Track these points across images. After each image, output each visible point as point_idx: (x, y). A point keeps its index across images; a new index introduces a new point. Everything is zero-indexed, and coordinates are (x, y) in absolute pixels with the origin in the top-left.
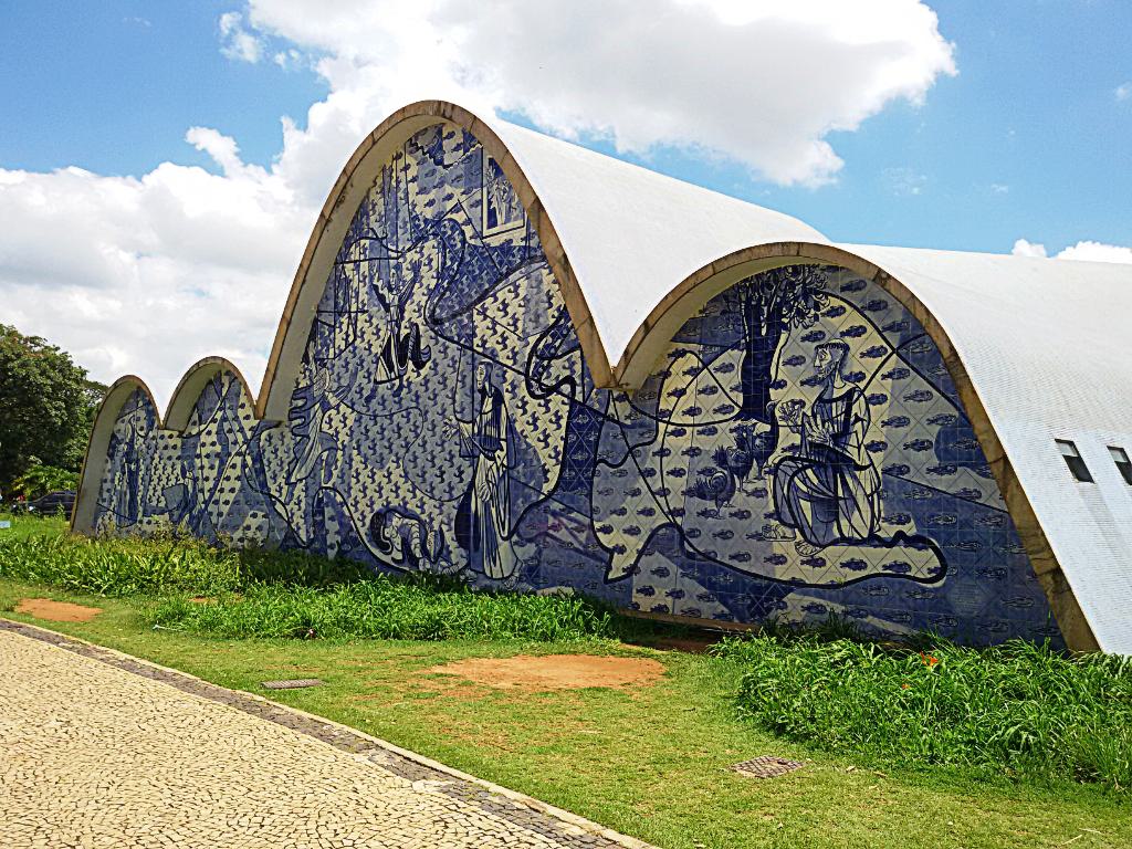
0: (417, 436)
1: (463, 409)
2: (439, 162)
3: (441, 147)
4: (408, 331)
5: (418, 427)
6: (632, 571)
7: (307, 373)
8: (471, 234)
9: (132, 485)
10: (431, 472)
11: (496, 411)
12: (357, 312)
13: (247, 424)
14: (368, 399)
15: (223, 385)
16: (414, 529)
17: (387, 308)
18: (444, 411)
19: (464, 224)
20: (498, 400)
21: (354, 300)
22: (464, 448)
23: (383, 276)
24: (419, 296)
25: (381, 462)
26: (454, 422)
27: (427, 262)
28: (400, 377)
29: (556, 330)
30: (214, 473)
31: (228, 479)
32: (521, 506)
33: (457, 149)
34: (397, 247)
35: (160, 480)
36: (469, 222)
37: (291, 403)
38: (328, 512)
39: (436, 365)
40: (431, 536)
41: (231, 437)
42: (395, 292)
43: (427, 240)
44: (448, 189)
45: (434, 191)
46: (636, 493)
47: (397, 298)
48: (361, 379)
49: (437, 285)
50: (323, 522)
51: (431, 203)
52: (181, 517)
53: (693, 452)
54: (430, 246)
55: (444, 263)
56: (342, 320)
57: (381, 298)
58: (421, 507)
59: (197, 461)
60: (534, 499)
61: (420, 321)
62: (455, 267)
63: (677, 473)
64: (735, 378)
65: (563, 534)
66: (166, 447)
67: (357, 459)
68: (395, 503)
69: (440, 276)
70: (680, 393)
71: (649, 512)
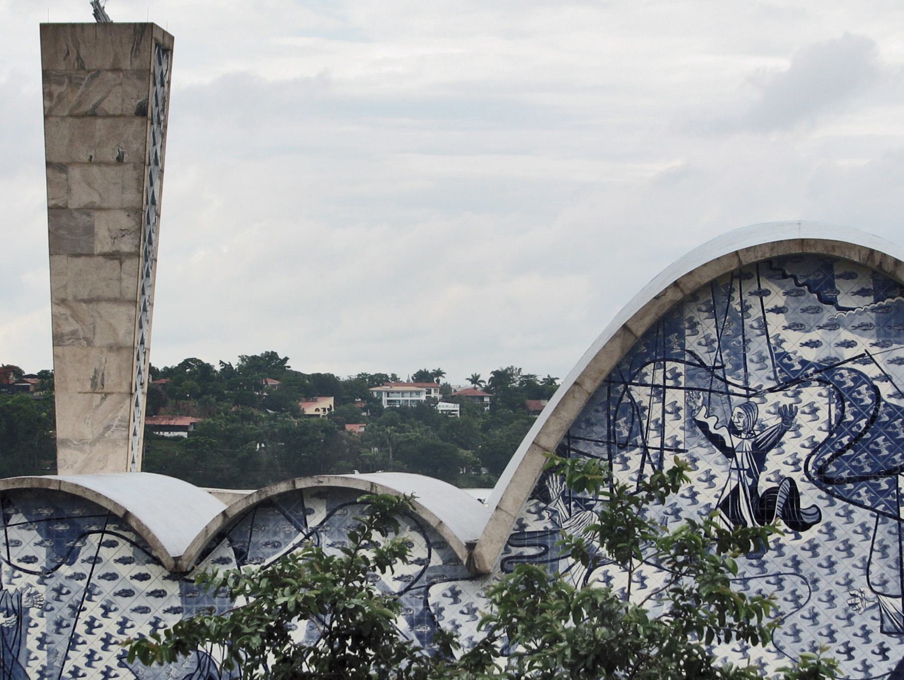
0: (799, 607)
1: (884, 583)
2: (833, 302)
3: (832, 286)
4: (776, 485)
5: (799, 597)
7: (545, 513)
8: (891, 392)
12: (662, 448)
15: (311, 512)
17: (729, 453)
18: (851, 581)
19: (876, 378)
21: (652, 434)
22: (888, 623)
23: (718, 411)
24: (793, 445)
26: (869, 594)
27: (807, 410)
33: (863, 292)
34: (746, 382)
36: (887, 378)
37: (507, 550)
39: (830, 530)
42: (743, 436)
43: (807, 384)
44: (845, 335)
45: (820, 331)
47: (748, 444)
49: (827, 440)
54: (813, 394)
55: (843, 417)
56: (627, 455)
57: (717, 441)
62: (863, 423)
66: (127, 593)
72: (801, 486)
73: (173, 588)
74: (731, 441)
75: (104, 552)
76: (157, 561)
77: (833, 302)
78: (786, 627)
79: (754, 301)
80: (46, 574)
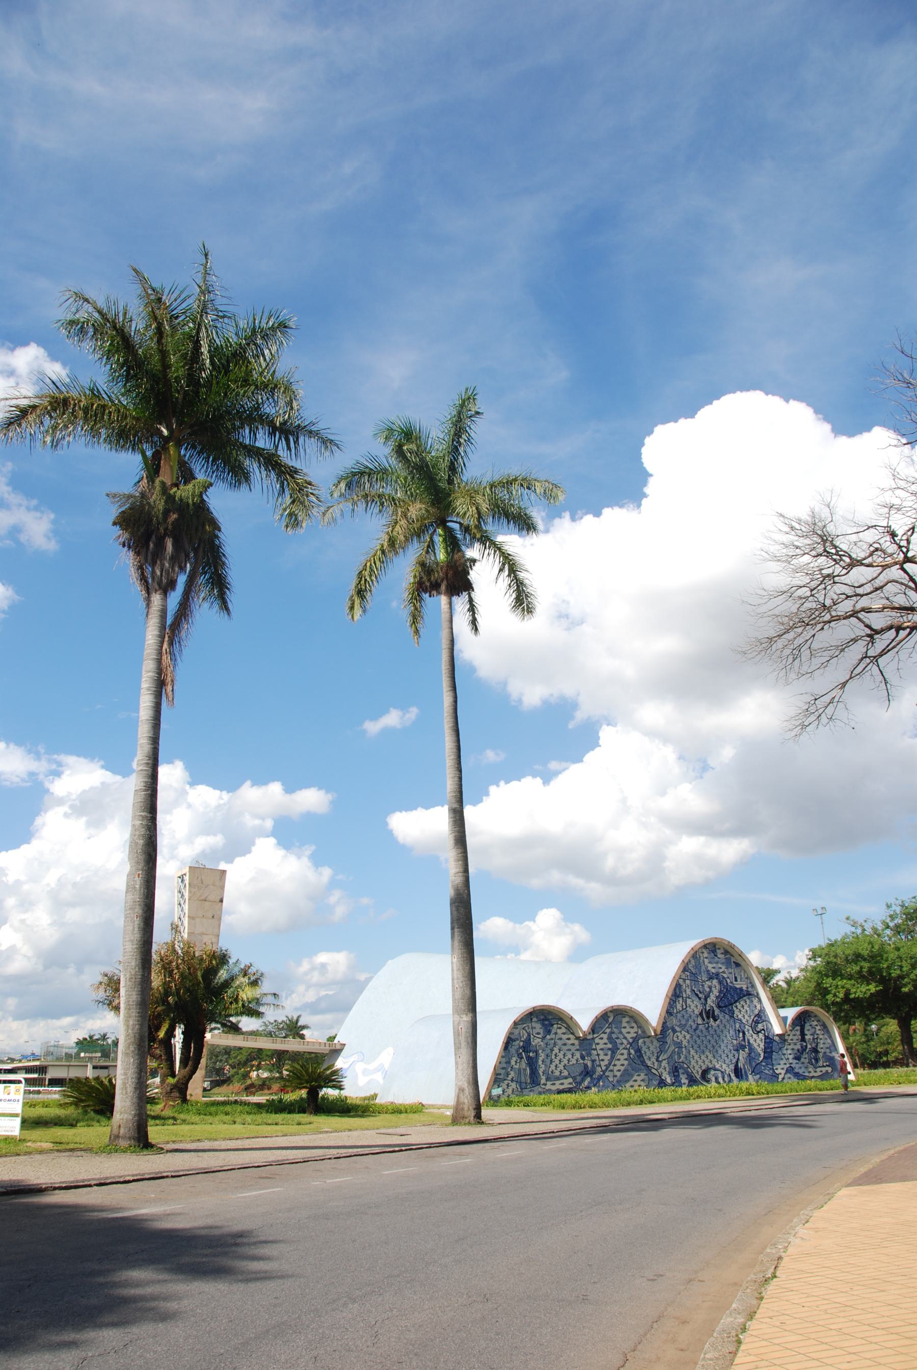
6: (783, 1079)
9: (532, 1063)
10: (724, 1056)
11: (744, 1036)
13: (628, 1036)
14: (695, 1030)
15: (609, 1017)
16: (720, 1075)
17: (700, 999)
20: (744, 1033)
24: (712, 997)
25: (703, 1052)
28: (708, 1023)
29: (758, 1015)
30: (609, 1057)
31: (619, 1060)
32: (754, 1064)
33: (722, 953)
35: (560, 1061)
36: (728, 978)
38: (681, 1071)
39: (721, 1021)
40: (726, 1076)
41: (618, 1041)
46: (782, 1059)
48: (690, 1022)
50: (679, 1075)
51: (714, 968)
52: (583, 1080)
53: (793, 1049)
54: (715, 982)
57: (697, 995)
58: (721, 1066)
59: (594, 1052)
60: (758, 1062)
61: (714, 1006)
63: (790, 1054)
64: (798, 1033)
65: (766, 1072)
66: (565, 1044)
67: (692, 1052)
68: (711, 1066)
69: (720, 992)
70: (789, 1035)
71: (785, 1064)
72: (715, 1008)
73: (576, 1042)
74: (700, 995)
75: (559, 1031)
76: (573, 1034)
77: (716, 956)
78: (715, 1050)
79: (701, 955)
80: (544, 1038)
